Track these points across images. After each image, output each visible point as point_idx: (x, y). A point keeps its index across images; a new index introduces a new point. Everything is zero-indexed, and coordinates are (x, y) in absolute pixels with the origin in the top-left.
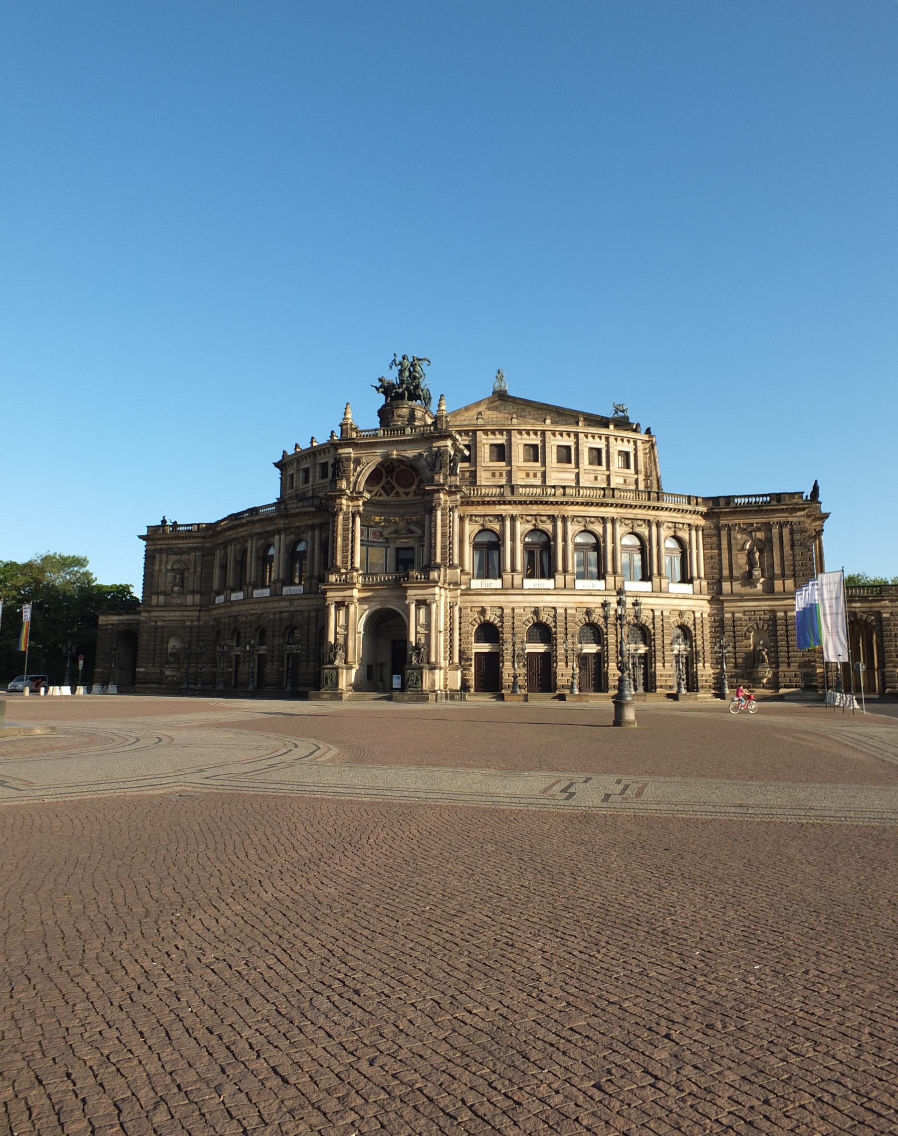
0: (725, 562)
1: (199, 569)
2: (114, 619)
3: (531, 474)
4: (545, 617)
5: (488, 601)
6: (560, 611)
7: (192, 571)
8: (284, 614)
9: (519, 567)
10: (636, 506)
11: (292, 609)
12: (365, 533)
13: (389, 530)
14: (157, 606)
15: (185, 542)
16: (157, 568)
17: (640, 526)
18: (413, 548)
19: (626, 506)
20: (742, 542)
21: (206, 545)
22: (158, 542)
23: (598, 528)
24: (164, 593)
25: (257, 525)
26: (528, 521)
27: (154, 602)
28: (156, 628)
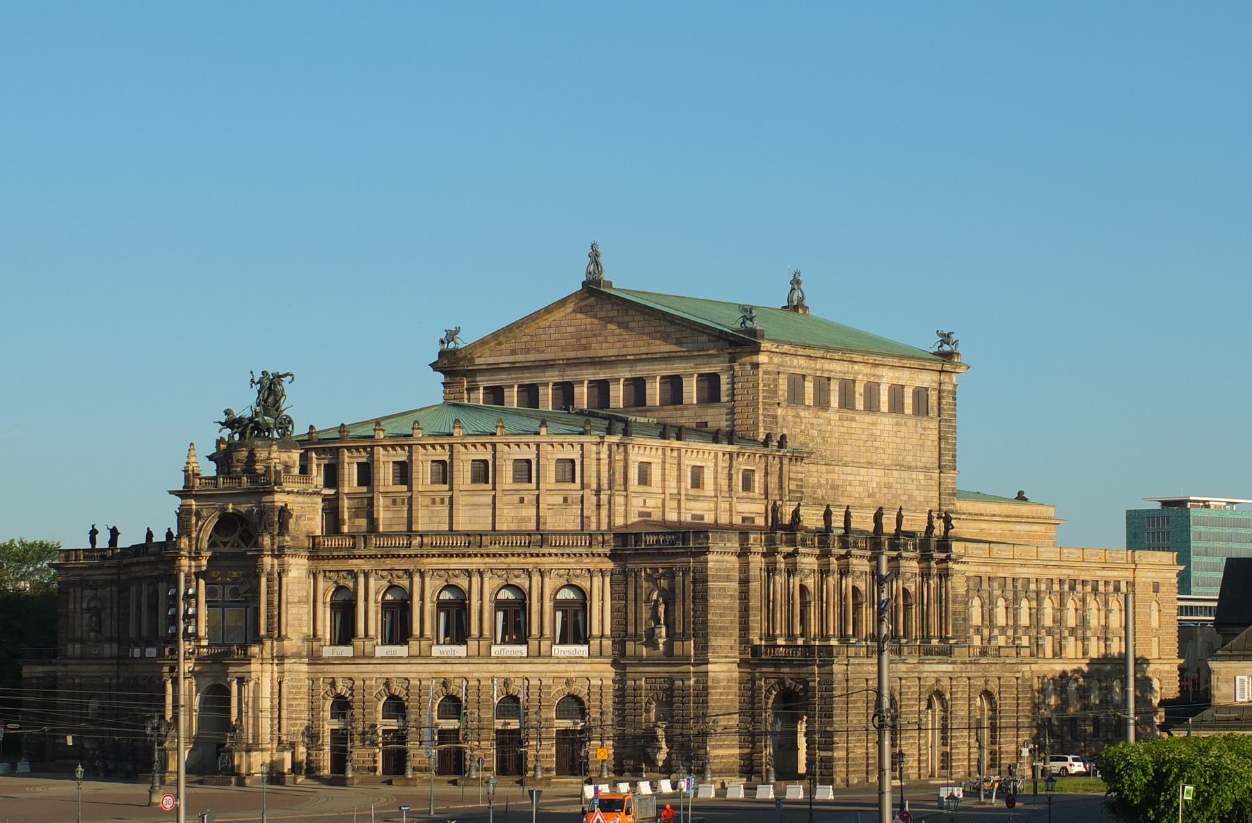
0: (631, 616)
2: (40, 669)
3: (438, 500)
4: (397, 689)
5: (339, 671)
6: (414, 682)
7: (108, 611)
9: (372, 632)
10: (507, 555)
12: (220, 592)
13: (245, 588)
14: (74, 658)
15: (99, 572)
16: (71, 606)
17: (517, 577)
19: (494, 555)
21: (122, 577)
23: (463, 583)
24: (82, 641)
26: (383, 577)
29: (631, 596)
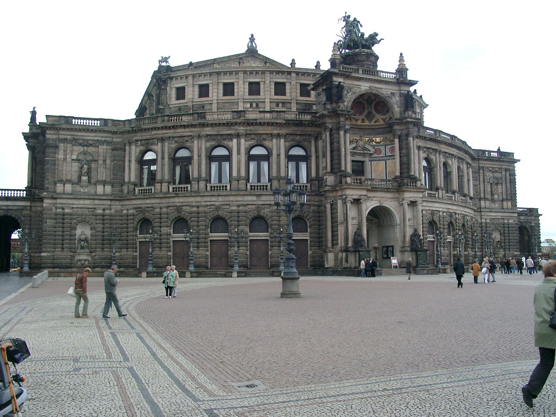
0: (482, 189)
1: (108, 162)
7: (101, 162)
8: (249, 206)
11: (262, 203)
14: (64, 194)
15: (92, 134)
16: (61, 156)
18: (363, 162)
20: (488, 178)
22: (61, 132)
24: (69, 181)
25: (206, 129)
27: (60, 188)
28: (64, 215)
29: (482, 179)
